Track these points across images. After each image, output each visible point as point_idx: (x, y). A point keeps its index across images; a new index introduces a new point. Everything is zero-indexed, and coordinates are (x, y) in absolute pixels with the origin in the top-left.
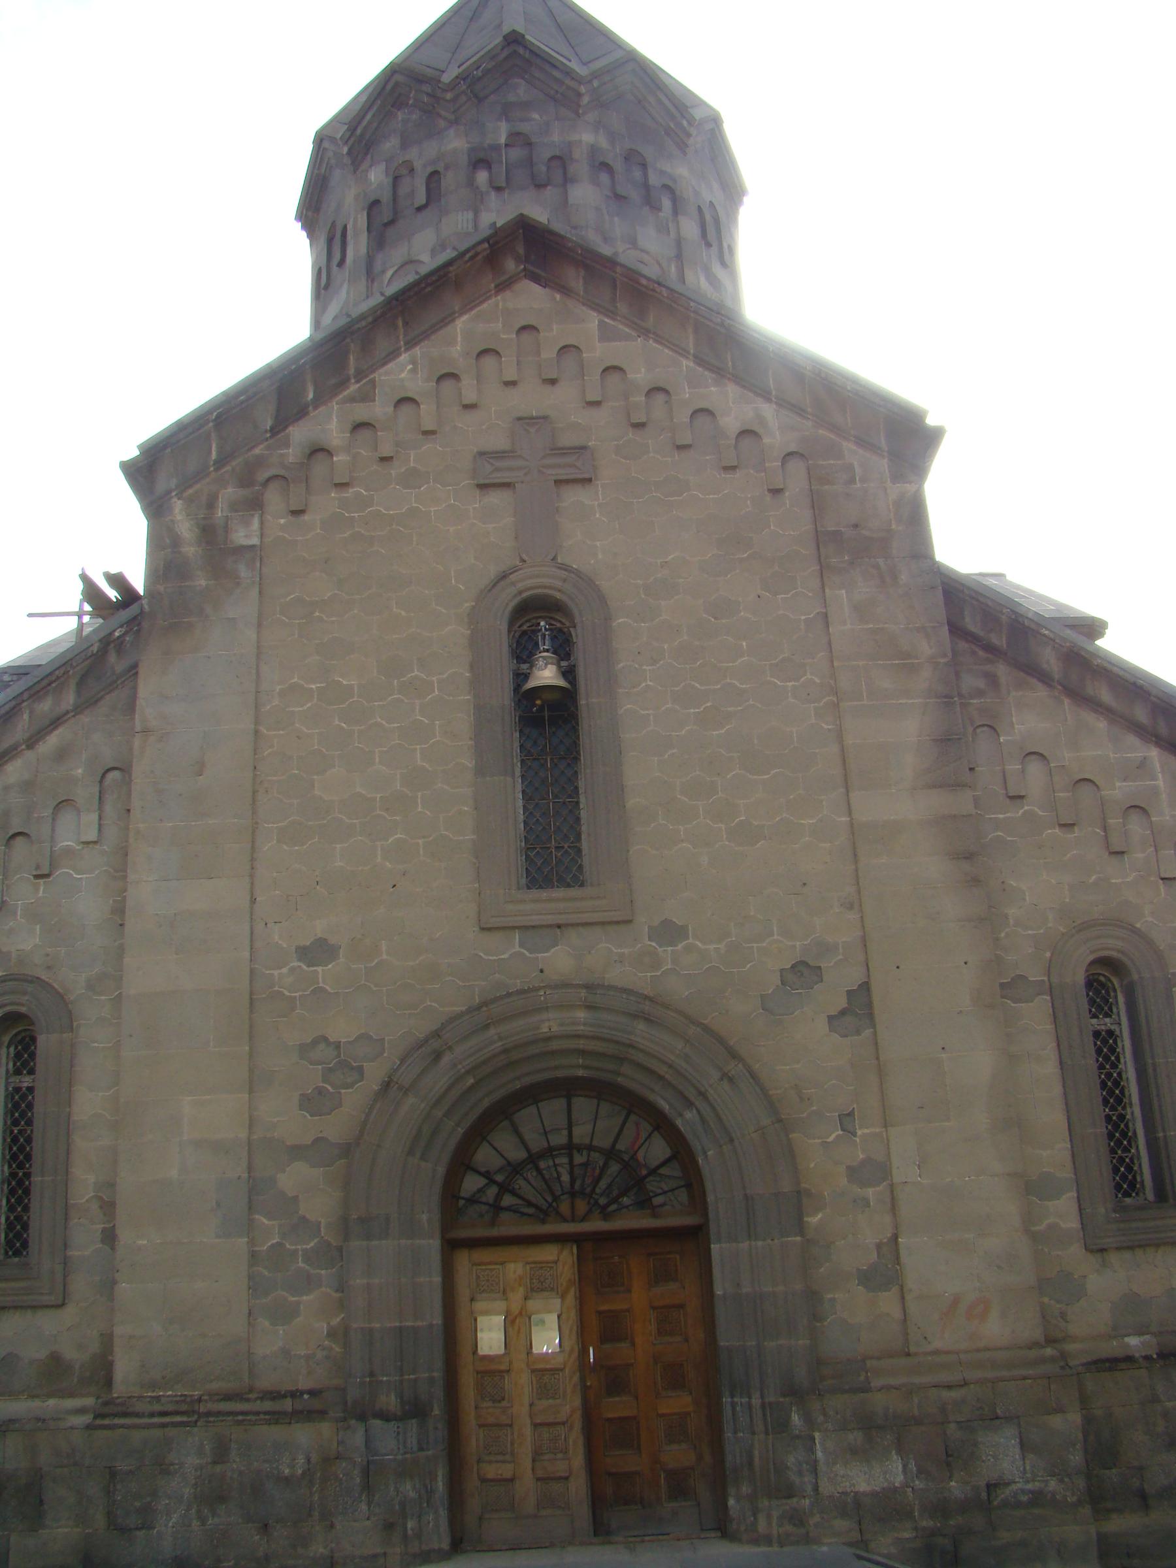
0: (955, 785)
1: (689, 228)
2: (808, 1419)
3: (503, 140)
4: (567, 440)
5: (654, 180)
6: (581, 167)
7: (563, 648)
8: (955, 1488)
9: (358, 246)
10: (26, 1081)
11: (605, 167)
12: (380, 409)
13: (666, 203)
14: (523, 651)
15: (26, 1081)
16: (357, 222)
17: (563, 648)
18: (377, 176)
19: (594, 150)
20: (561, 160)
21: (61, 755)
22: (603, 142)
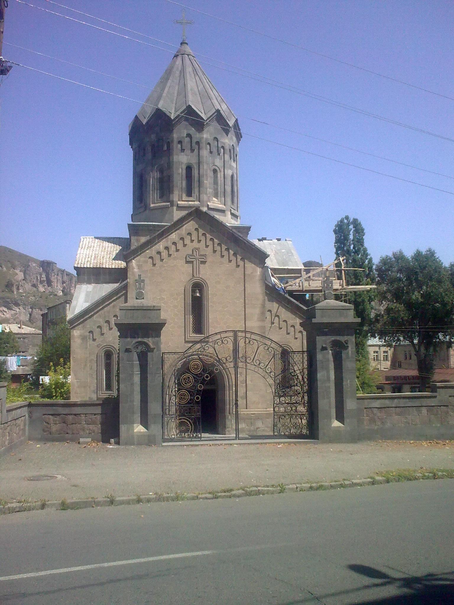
0: (263, 321)
1: (227, 157)
2: (231, 417)
3: (185, 135)
4: (202, 253)
5: (220, 146)
6: (203, 145)
7: (201, 292)
8: (252, 428)
9: (149, 156)
10: (108, 361)
11: (209, 144)
12: (169, 244)
13: (222, 150)
14: (193, 291)
15: (108, 361)
16: (149, 148)
17: (201, 292)
18: (153, 137)
19: (207, 139)
20: (198, 143)
21: (114, 306)
22: (209, 137)
